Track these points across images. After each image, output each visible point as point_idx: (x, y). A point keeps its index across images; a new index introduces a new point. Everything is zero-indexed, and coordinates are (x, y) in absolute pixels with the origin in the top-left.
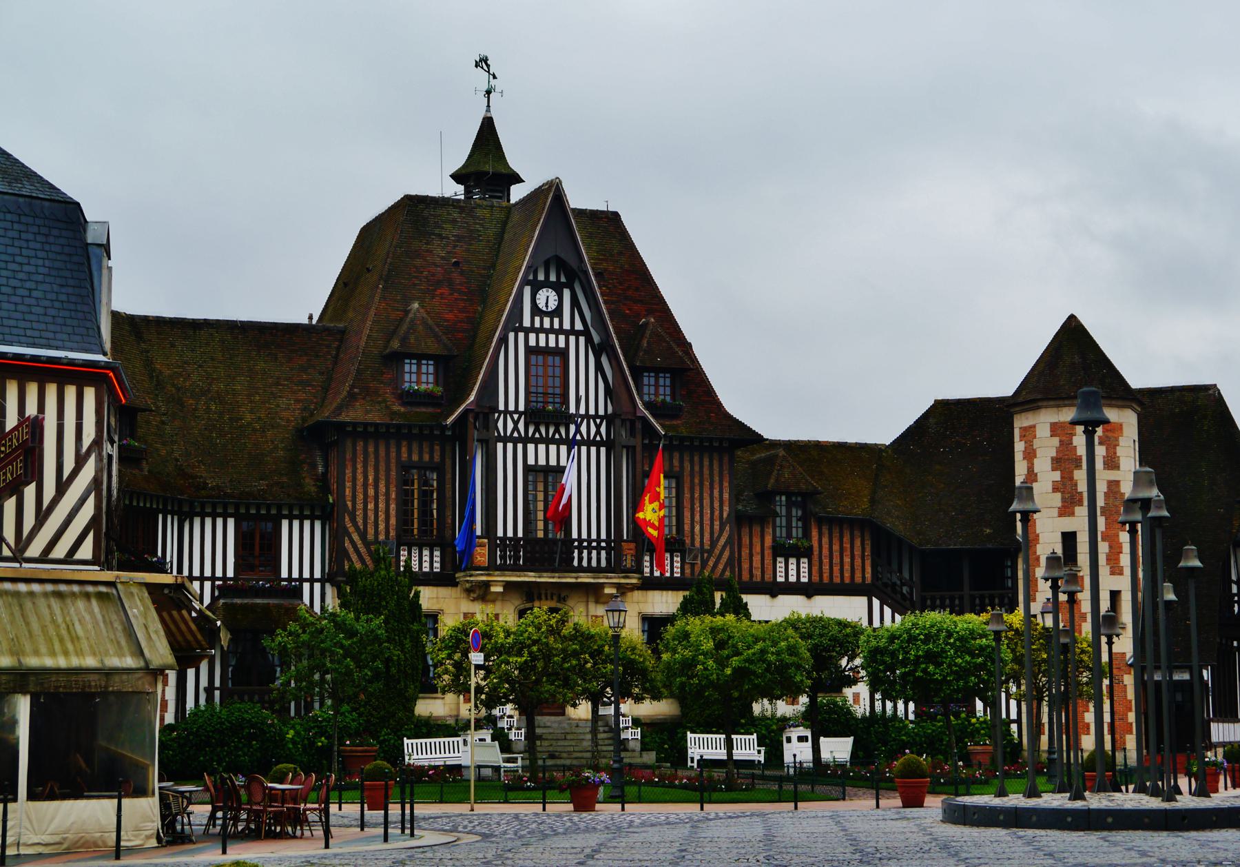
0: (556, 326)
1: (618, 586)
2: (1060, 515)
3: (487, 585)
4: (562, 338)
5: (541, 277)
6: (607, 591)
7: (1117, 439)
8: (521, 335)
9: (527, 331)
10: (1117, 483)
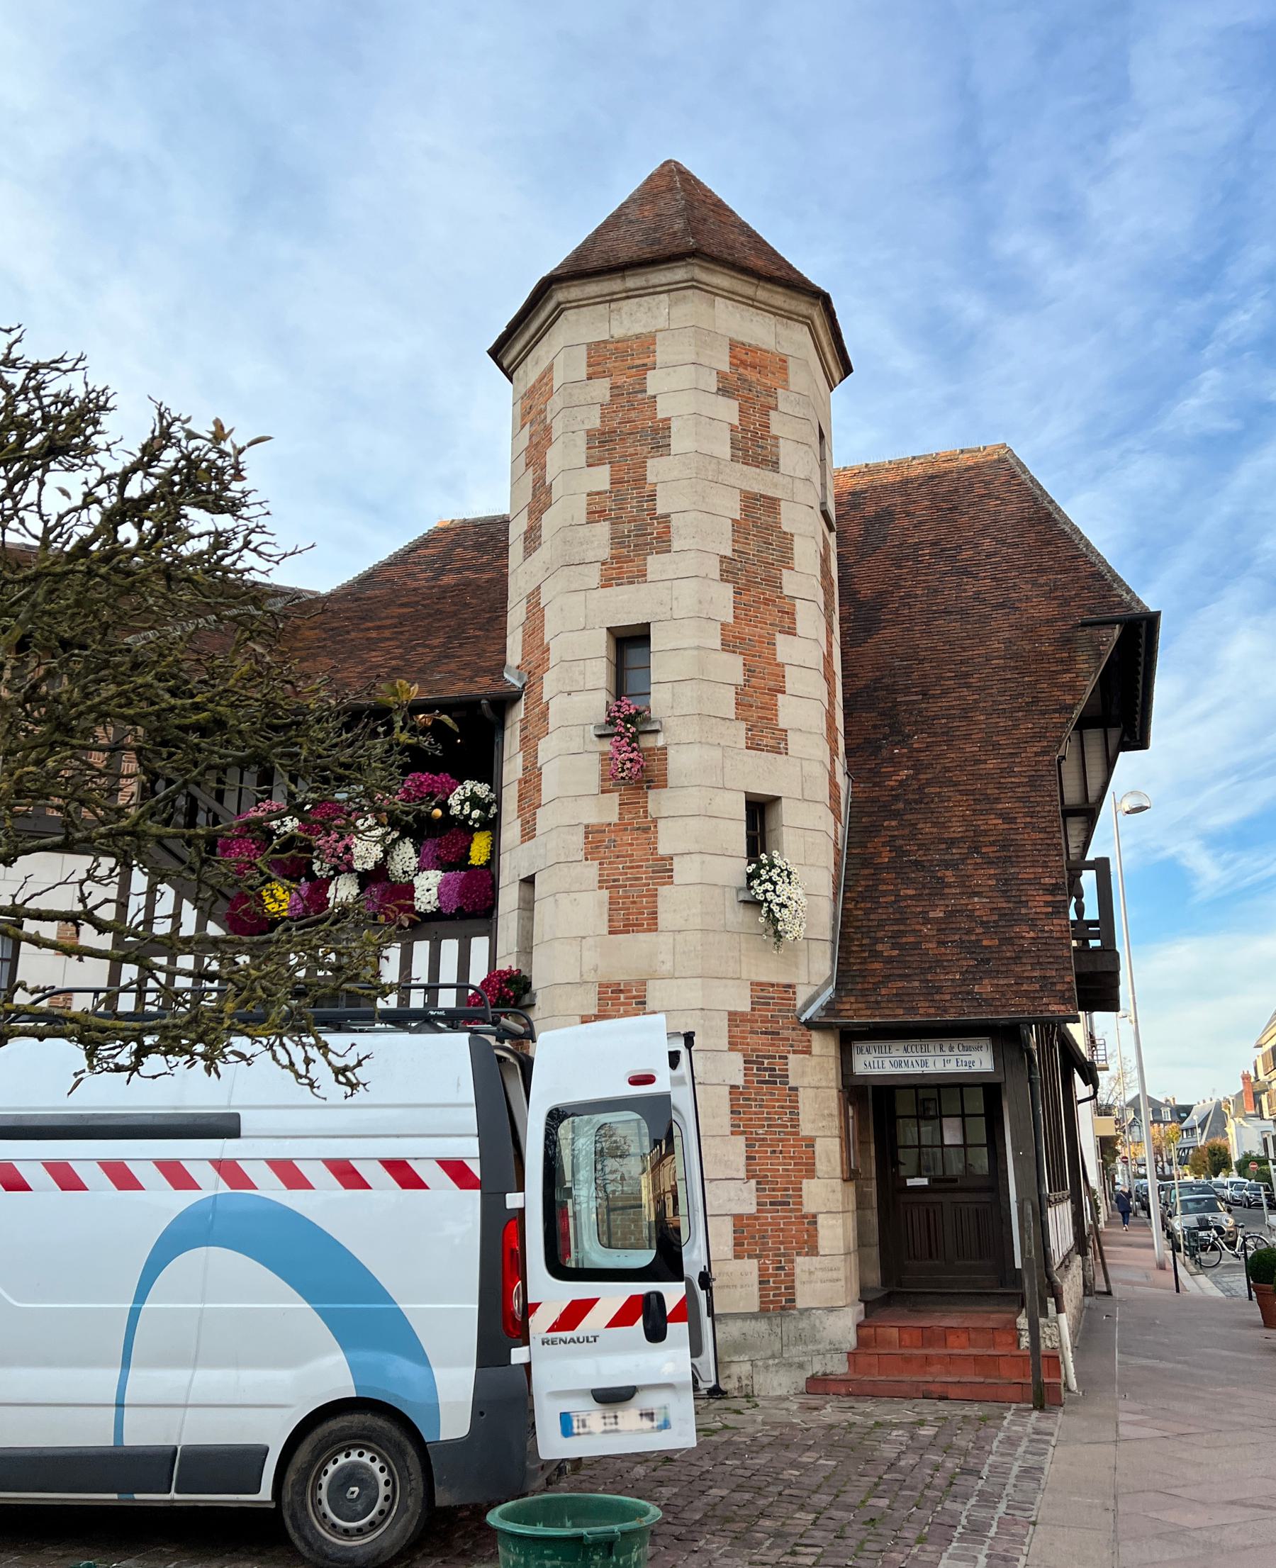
2: (607, 583)
7: (771, 392)
10: (772, 504)
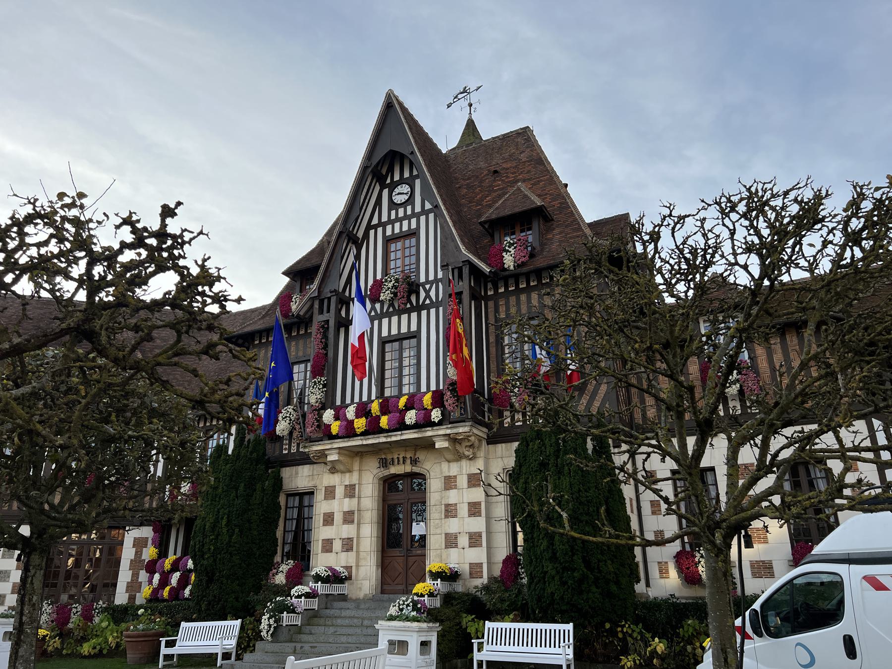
0: (409, 212)
1: (454, 440)
3: (323, 454)
4: (414, 221)
5: (397, 177)
6: (440, 444)
8: (380, 230)
9: (384, 225)
